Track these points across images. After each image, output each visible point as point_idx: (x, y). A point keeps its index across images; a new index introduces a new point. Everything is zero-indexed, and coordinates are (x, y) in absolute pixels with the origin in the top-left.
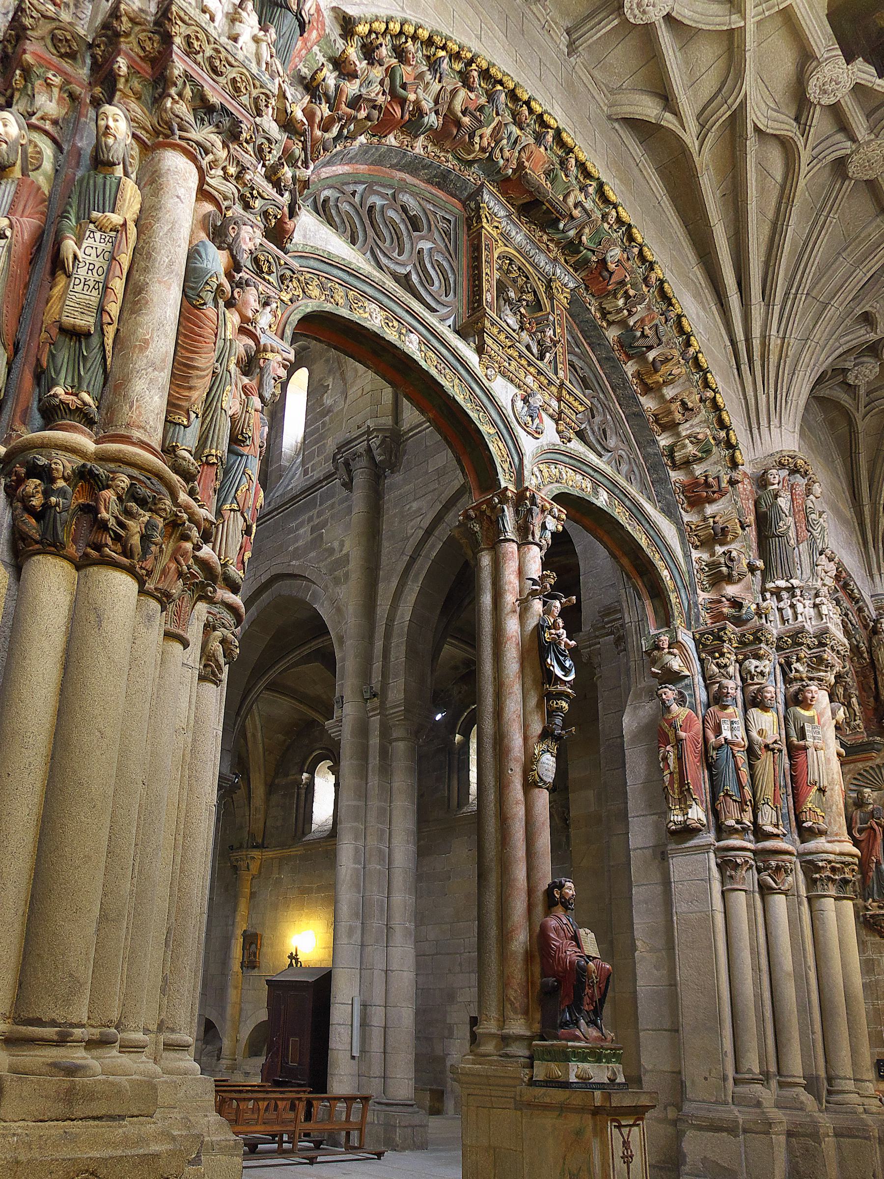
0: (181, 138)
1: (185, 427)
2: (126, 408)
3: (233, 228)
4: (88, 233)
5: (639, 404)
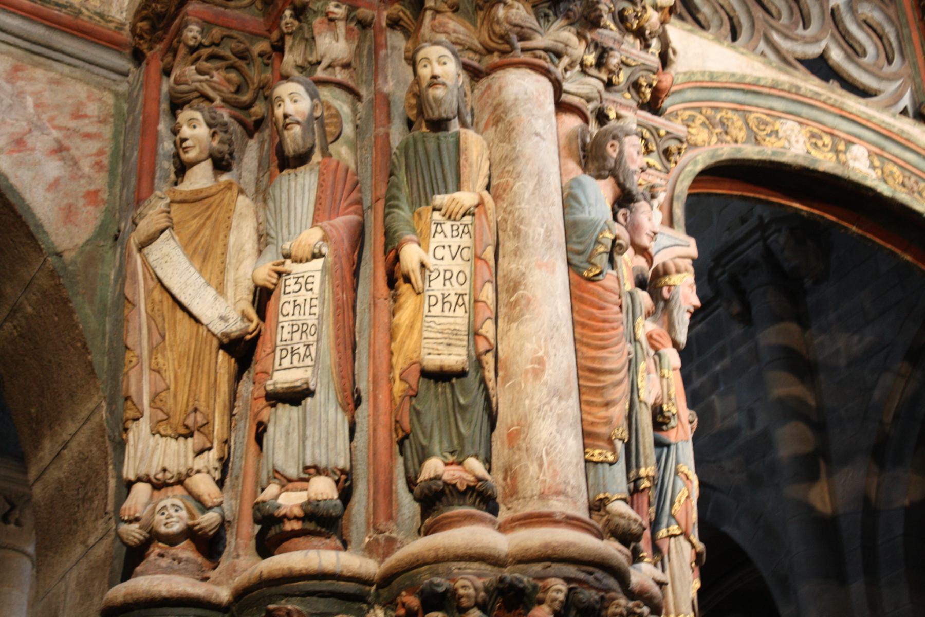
0: (524, 50)
1: (611, 464)
2: (533, 469)
3: (612, 145)
4: (433, 227)
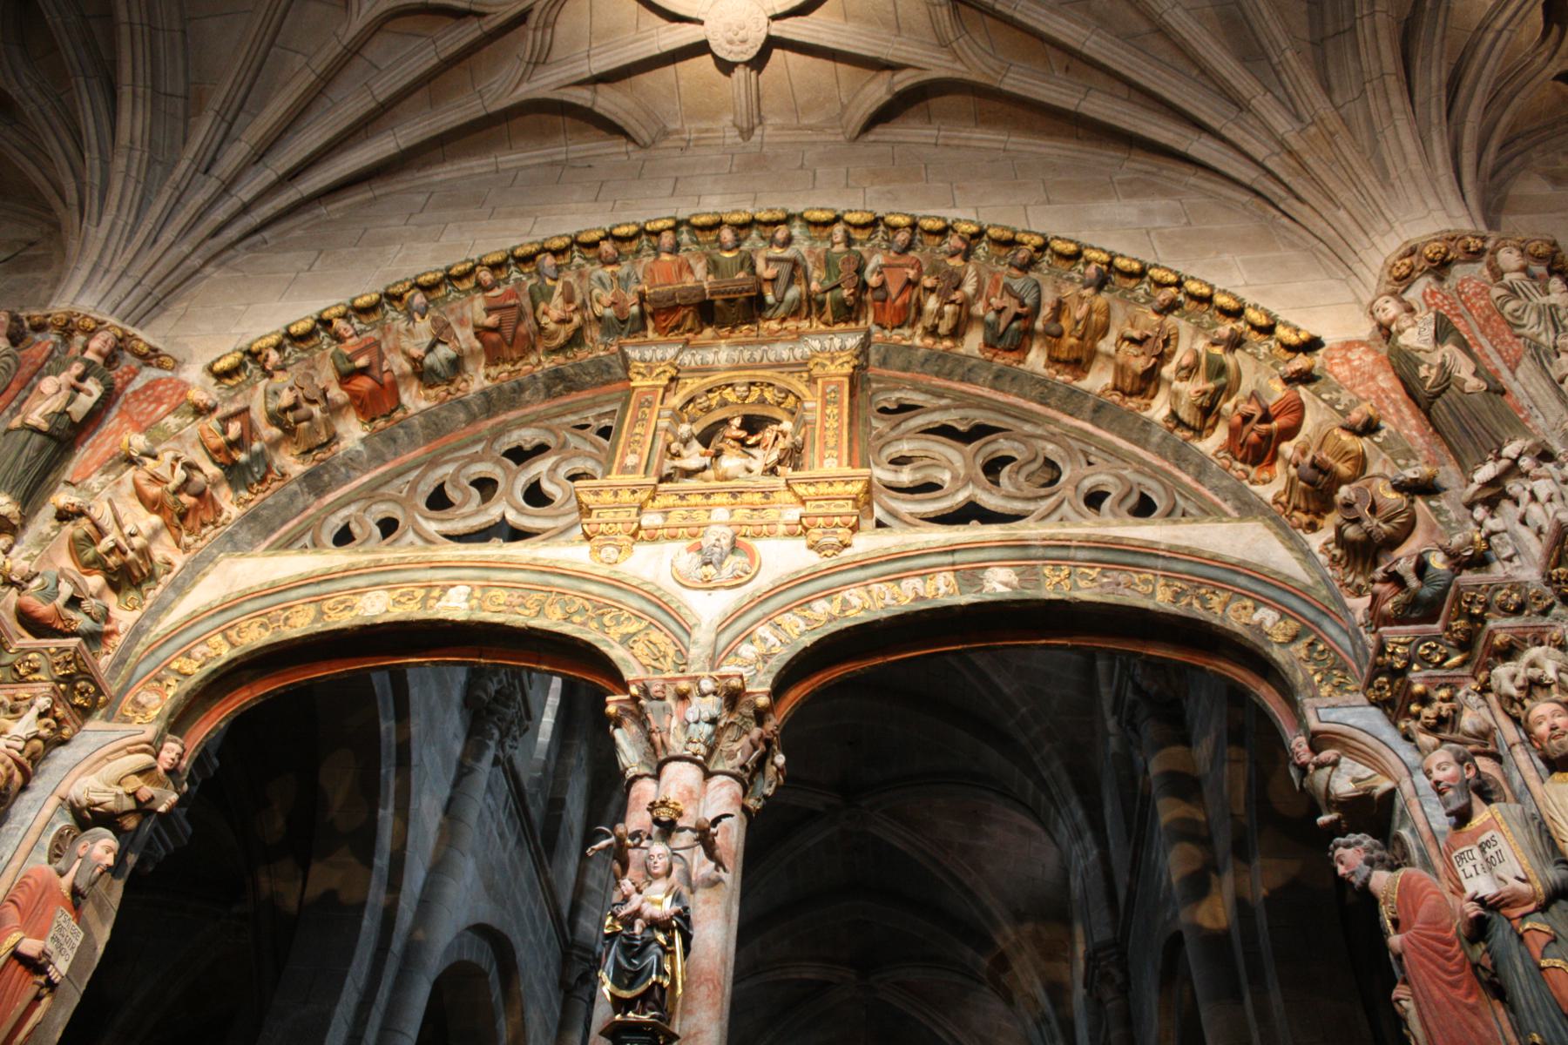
5: (1085, 394)
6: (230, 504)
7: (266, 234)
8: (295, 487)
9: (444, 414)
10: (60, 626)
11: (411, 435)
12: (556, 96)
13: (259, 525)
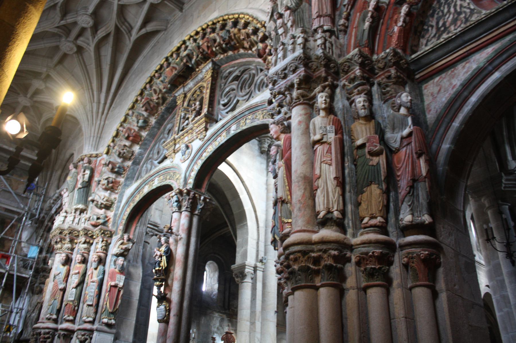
6: (121, 180)
7: (113, 106)
8: (132, 167)
9: (152, 132)
10: (98, 224)
11: (149, 140)
12: (138, 36)
13: (130, 179)
